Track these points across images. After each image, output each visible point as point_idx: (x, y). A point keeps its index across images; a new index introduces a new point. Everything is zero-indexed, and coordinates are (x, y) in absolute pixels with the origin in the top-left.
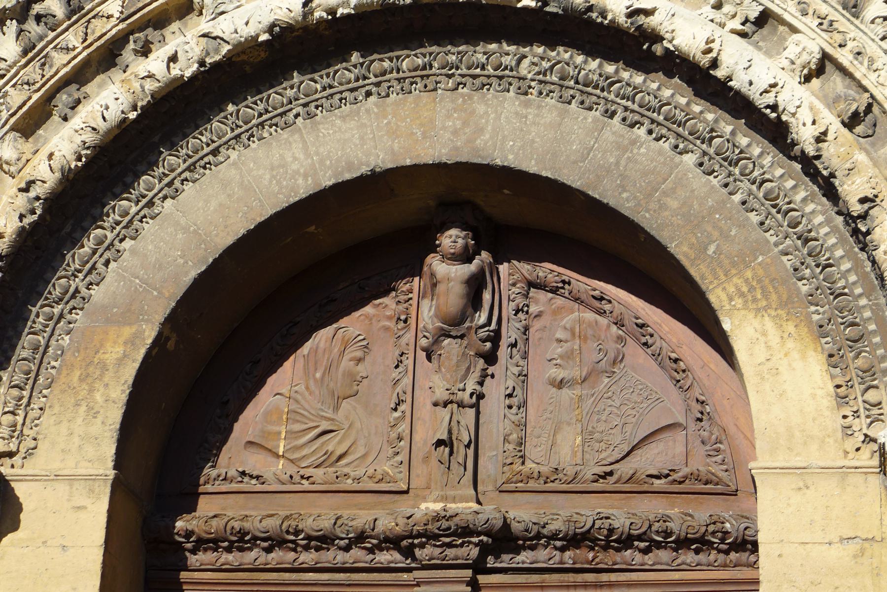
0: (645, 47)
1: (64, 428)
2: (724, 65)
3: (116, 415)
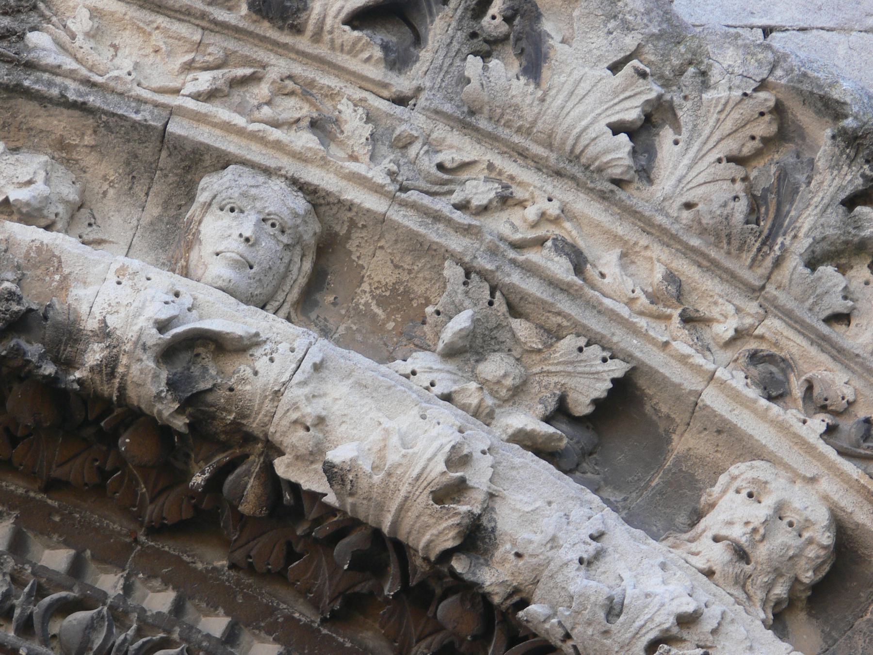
0: (198, 479)
2: (505, 549)
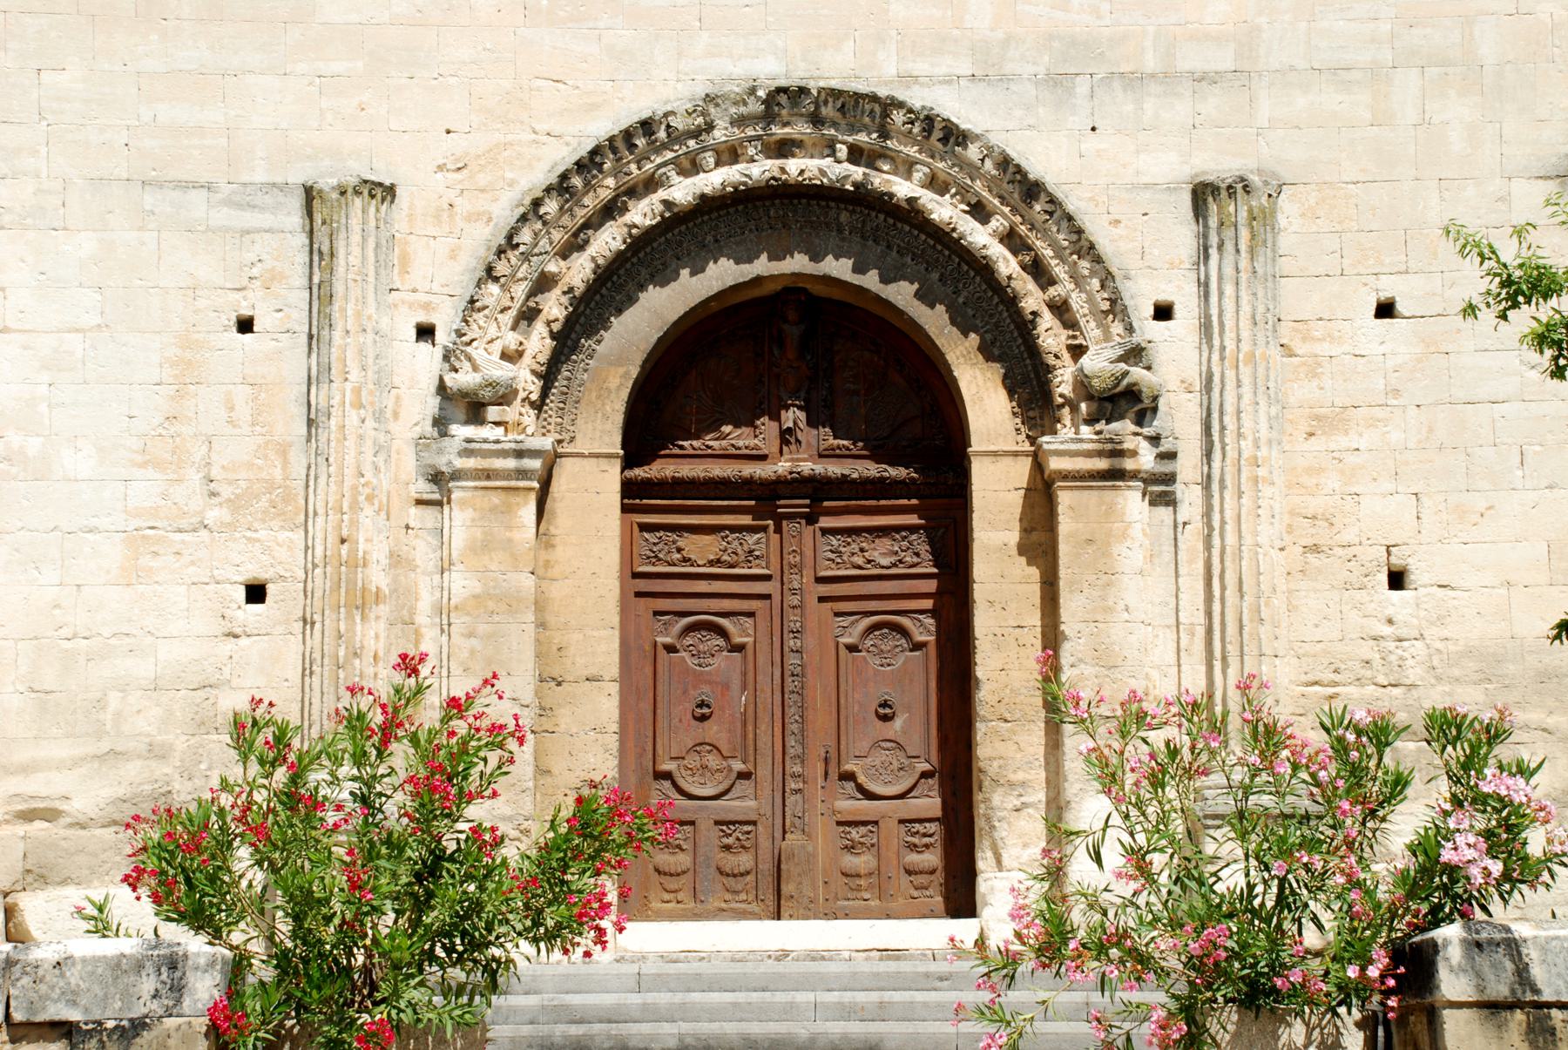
1: (590, 426)
3: (619, 419)
